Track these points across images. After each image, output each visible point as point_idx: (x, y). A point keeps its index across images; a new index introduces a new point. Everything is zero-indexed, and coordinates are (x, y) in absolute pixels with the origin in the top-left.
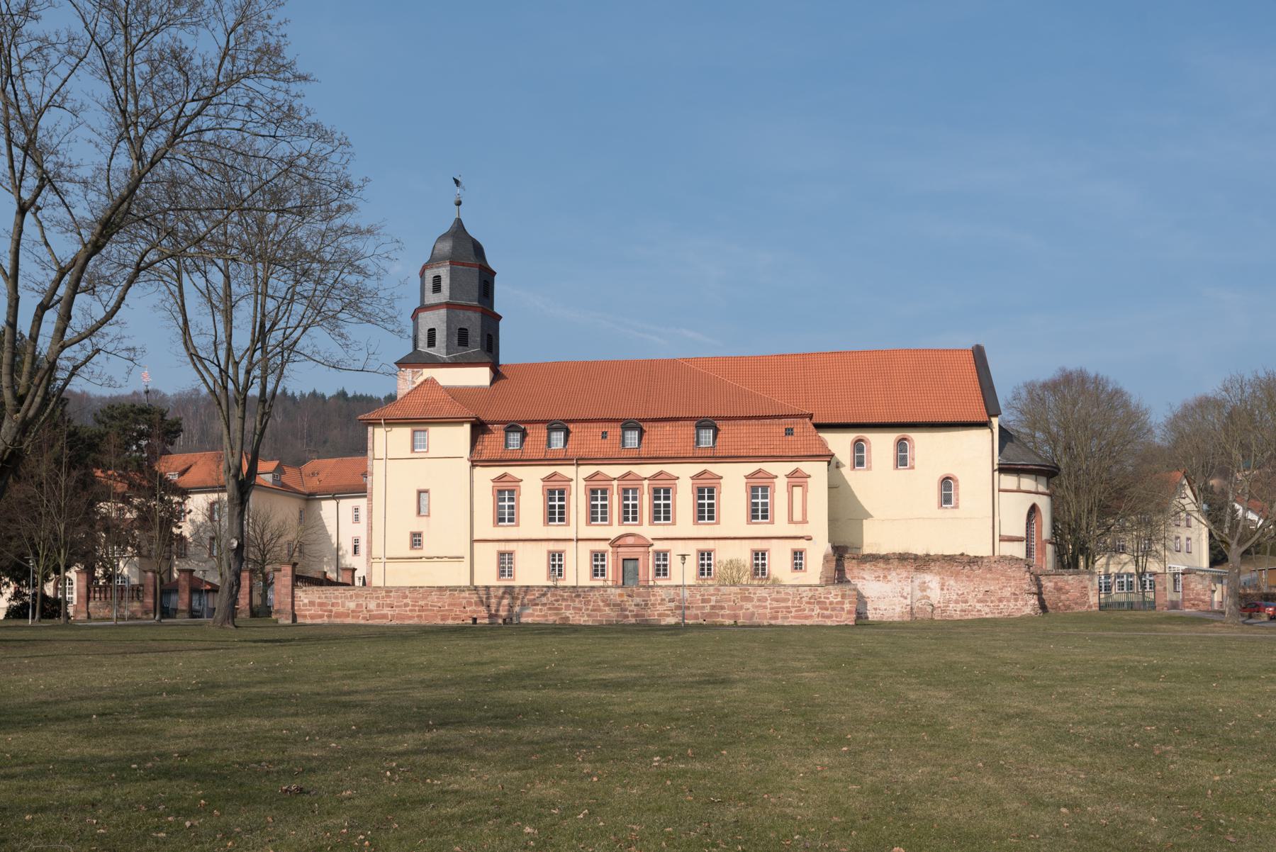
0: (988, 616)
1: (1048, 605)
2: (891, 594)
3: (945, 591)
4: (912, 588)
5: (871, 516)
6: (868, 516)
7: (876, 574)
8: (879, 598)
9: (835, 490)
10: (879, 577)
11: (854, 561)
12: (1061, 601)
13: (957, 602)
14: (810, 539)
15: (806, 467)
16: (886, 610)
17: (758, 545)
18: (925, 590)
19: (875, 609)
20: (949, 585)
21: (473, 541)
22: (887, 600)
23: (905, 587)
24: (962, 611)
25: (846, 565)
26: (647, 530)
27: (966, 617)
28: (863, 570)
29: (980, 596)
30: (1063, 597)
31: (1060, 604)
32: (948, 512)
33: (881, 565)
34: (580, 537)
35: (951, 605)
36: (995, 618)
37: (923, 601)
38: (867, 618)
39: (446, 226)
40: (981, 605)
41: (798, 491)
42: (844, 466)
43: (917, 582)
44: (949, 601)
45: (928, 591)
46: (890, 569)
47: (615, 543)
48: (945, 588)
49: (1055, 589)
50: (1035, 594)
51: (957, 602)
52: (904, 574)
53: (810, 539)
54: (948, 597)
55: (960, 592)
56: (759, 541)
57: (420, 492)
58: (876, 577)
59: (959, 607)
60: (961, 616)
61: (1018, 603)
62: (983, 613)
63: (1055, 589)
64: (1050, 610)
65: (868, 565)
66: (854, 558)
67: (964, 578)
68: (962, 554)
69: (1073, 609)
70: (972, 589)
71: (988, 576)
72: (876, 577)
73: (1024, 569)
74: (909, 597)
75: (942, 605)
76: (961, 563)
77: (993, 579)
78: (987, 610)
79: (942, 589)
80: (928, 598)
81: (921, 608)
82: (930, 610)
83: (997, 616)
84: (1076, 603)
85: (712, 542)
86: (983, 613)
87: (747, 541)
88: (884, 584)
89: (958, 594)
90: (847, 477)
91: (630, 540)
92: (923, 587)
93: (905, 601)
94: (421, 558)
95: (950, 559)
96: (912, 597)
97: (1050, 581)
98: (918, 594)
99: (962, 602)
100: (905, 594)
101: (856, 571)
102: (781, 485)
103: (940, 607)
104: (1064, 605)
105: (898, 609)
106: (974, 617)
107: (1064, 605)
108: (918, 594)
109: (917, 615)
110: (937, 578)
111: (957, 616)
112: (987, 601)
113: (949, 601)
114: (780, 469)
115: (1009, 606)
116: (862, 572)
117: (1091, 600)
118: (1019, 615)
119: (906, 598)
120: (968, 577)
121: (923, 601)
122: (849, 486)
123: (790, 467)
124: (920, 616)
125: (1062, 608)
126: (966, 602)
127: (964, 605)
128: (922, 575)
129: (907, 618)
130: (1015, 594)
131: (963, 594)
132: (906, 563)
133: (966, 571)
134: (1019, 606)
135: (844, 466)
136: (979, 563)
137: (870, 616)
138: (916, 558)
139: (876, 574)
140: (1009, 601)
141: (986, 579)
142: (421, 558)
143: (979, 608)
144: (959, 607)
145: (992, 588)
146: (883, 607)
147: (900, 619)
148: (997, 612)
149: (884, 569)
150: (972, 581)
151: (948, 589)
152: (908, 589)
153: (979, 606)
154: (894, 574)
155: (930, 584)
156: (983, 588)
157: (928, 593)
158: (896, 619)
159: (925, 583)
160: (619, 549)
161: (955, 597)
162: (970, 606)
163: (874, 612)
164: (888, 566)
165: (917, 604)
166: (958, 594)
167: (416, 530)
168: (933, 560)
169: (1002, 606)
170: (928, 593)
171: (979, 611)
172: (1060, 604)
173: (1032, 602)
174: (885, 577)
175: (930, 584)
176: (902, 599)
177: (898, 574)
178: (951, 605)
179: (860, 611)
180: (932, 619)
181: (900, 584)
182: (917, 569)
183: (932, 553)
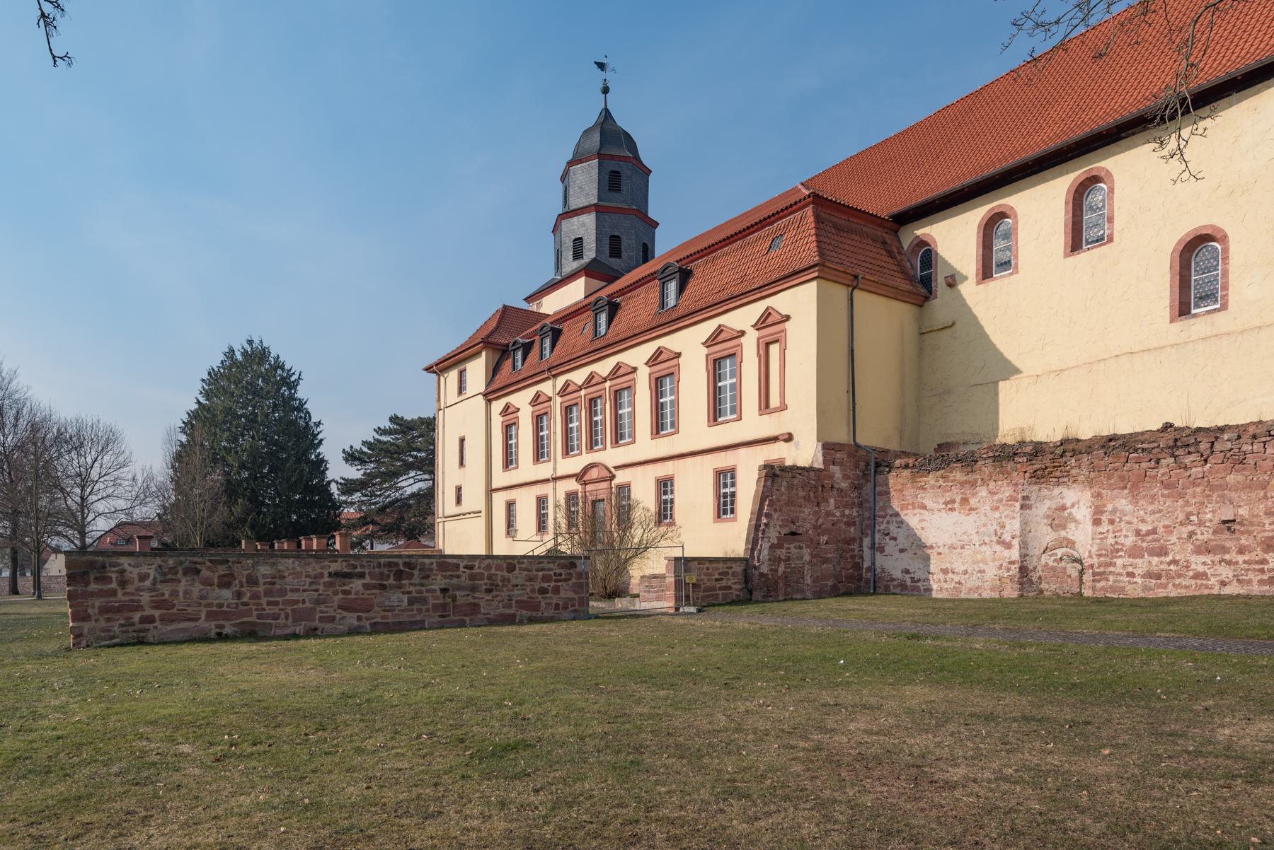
2: (976, 539)
3: (1105, 527)
4: (1025, 523)
5: (1017, 371)
6: (1010, 370)
7: (948, 496)
8: (952, 547)
9: (948, 332)
10: (953, 501)
11: (906, 473)
13: (1135, 552)
14: (789, 438)
15: (781, 302)
16: (965, 572)
17: (723, 460)
18: (1064, 527)
19: (945, 571)
20: (1114, 511)
21: (490, 491)
22: (966, 552)
23: (1007, 522)
24: (1149, 575)
25: (891, 481)
26: (611, 456)
27: (1161, 593)
28: (923, 488)
29: (1204, 535)
32: (1200, 325)
33: (958, 475)
34: (559, 474)
35: (1119, 562)
36: (1248, 597)
37: (1059, 552)
38: (929, 590)
39: (591, 118)
40: (1208, 559)
41: (775, 350)
42: (966, 278)
43: (1042, 508)
44: (1115, 551)
45: (1072, 526)
46: (973, 484)
47: (580, 477)
48: (1104, 518)
51: (1135, 552)
52: (1007, 492)
53: (789, 438)
54: (1111, 540)
55: (1144, 528)
56: (723, 454)
57: (462, 441)
58: (946, 503)
59: (1141, 565)
60: (1146, 588)
62: (1213, 581)
65: (931, 479)
66: (907, 466)
67: (1157, 490)
68: (1167, 427)
70: (1181, 517)
71: (1231, 478)
72: (946, 503)
74: (1016, 542)
75: (1095, 560)
76: (1150, 451)
77: (1248, 487)
78: (1226, 572)
79: (1097, 522)
80: (1071, 544)
81: (1053, 569)
82: (1075, 574)
85: (670, 464)
86: (1213, 581)
87: (698, 459)
88: (962, 518)
89: (1138, 533)
90: (970, 302)
91: (594, 473)
92: (1059, 519)
93: (1006, 553)
94: (459, 515)
95: (1115, 445)
96: (1024, 545)
98: (1045, 535)
99: (1153, 553)
100: (1007, 537)
101: (909, 492)
102: (749, 345)
103: (1092, 566)
105: (991, 571)
106: (1183, 592)
108: (1045, 535)
109: (1044, 586)
110: (1087, 495)
111: (1135, 589)
112: (1225, 550)
113: (1115, 551)
114: (743, 318)
116: (921, 494)
119: (1008, 546)
120: (1167, 486)
121: (1059, 552)
122: (975, 318)
123: (756, 310)
124: (1049, 587)
126: (1162, 552)
127: (1155, 560)
128: (1057, 491)
129: (1011, 592)
131: (1154, 531)
132: (1009, 466)
133: (1162, 471)
135: (966, 278)
136: (1204, 446)
137: (935, 587)
138: (1038, 450)
139: (948, 496)
141: (1226, 486)
142: (459, 515)
143: (1201, 569)
144: (1141, 565)
146: (959, 567)
147: (996, 595)
149: (962, 484)
150: (1181, 496)
151: (1111, 522)
152: (1014, 526)
153: (1199, 563)
154: (983, 492)
155: (1074, 511)
156: (1215, 513)
157: (1072, 532)
158: (986, 594)
159: (1063, 508)
160: (589, 488)
161: (1130, 540)
162: (1175, 562)
163: (942, 576)
164: (971, 477)
165: (1044, 559)
166: (1138, 533)
167: (458, 484)
168: (1075, 453)
170: (1072, 532)
171: (1197, 576)
174: (965, 501)
175: (1074, 511)
176: (998, 548)
177: (992, 493)
178: (1119, 562)
179: (916, 576)
180: (1080, 594)
181: (997, 515)
182: (1038, 477)
183: (1086, 433)
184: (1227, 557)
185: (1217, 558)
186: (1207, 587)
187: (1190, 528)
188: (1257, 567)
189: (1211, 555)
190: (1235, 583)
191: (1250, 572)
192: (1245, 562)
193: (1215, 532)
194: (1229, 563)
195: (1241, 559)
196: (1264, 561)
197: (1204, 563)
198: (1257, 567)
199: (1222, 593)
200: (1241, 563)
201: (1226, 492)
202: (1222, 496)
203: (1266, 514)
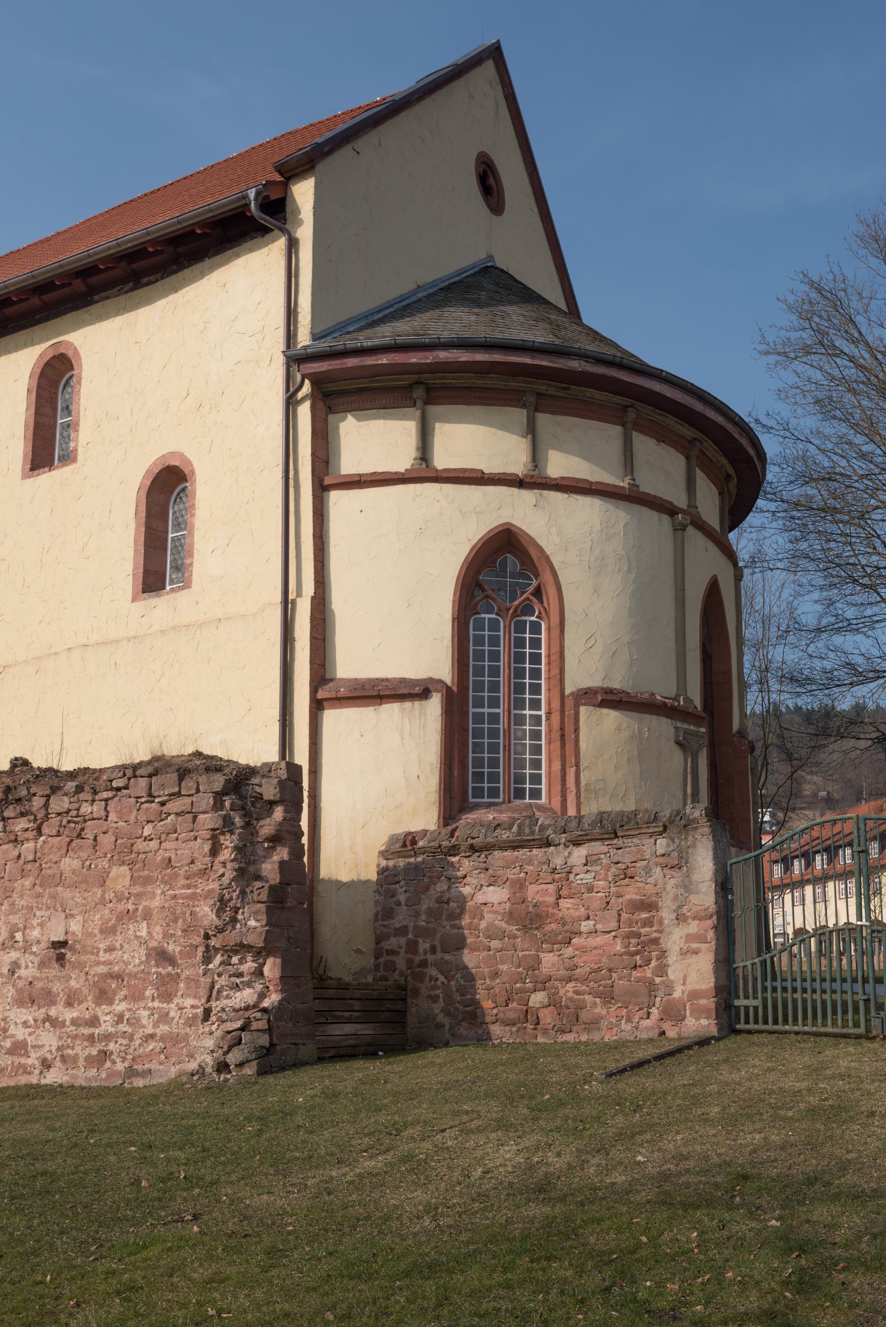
0: (53, 1077)
1: (487, 1004)
12: (542, 984)
30: (549, 961)
31: (537, 999)
49: (510, 917)
50: (261, 953)
61: (172, 1009)
63: (510, 917)
64: (496, 1030)
69: (593, 1024)
73: (208, 820)
78: (49, 1040)
83: (83, 1076)
84: (608, 996)
97: (493, 882)
104: (554, 1002)
107: (554, 1002)
115: (135, 1022)
117: (674, 973)
118: (173, 1072)
125: (547, 1017)
130: (163, 956)
134: (177, 1026)
140: (136, 996)
143: (20, 1033)
145: (75, 926)
148: (81, 1051)
169: (107, 1025)
171: (19, 1048)
172: (537, 999)
173: (247, 996)
184: (53, 1012)
185: (41, 1014)
186: (25, 1070)
187: (14, 955)
188: (86, 1031)
189: (35, 1007)
190: (58, 1063)
191: (78, 1042)
192: (74, 1022)
193: (42, 965)
194: (55, 1023)
195: (69, 1015)
196: (94, 1022)
197: (25, 1024)
198: (86, 1031)
199: (43, 1082)
200: (68, 1023)
201: (59, 889)
202: (54, 897)
203: (102, 931)
